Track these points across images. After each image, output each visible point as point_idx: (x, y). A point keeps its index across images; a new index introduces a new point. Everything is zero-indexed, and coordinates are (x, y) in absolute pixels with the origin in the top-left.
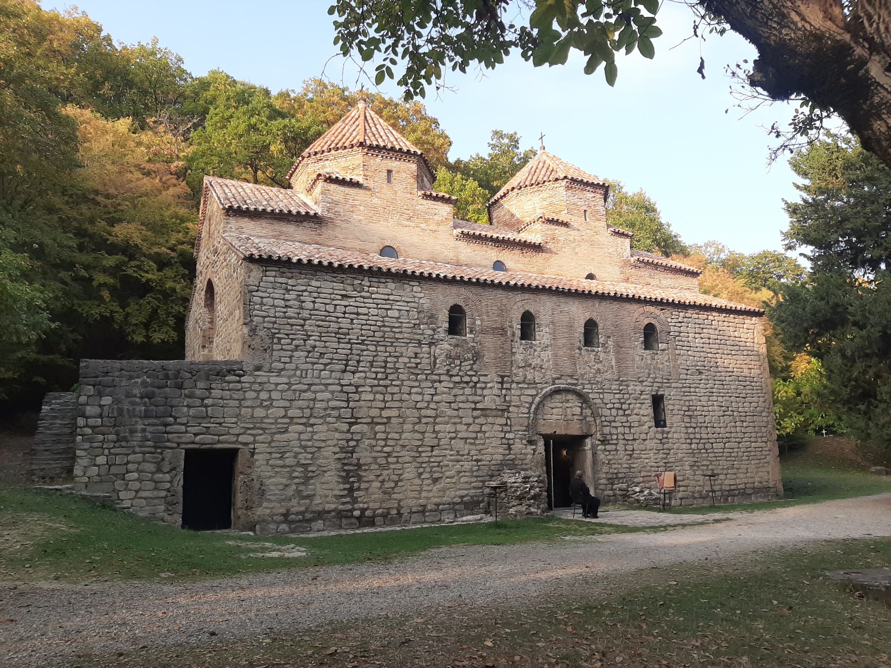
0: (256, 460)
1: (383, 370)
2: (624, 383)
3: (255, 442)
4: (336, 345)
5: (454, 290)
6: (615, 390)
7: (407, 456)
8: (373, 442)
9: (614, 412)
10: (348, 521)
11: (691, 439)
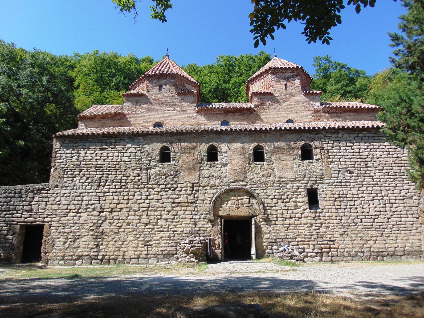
0: (52, 230)
1: (119, 184)
2: (283, 182)
3: (51, 221)
4: (95, 173)
6: (277, 187)
8: (112, 221)
9: (275, 201)
10: (96, 261)
11: (342, 217)
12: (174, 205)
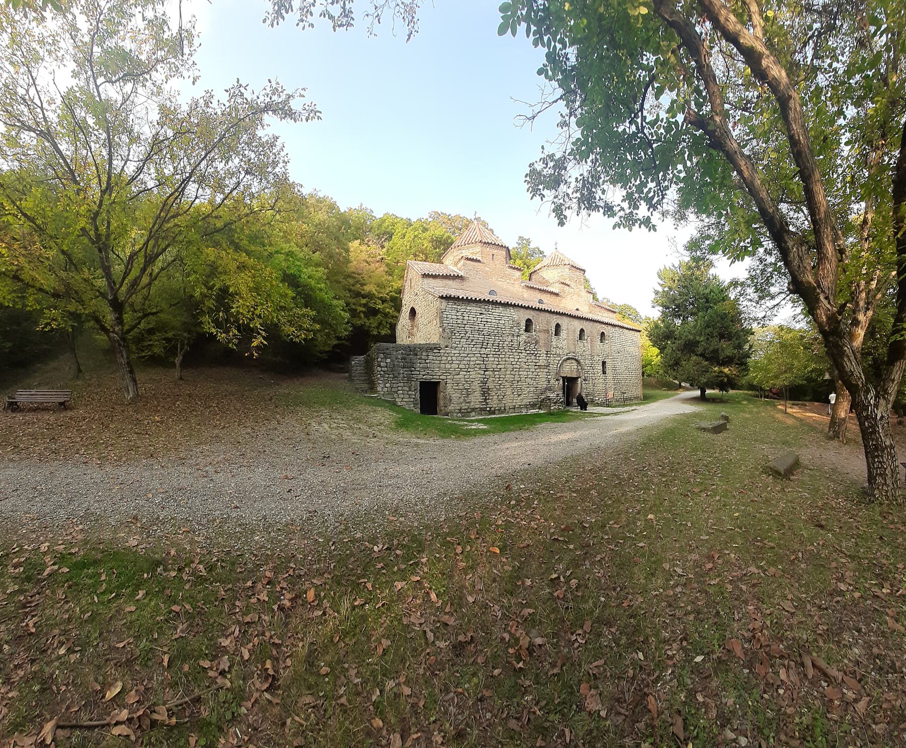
5: (528, 311)
7: (508, 385)
12: (536, 367)
